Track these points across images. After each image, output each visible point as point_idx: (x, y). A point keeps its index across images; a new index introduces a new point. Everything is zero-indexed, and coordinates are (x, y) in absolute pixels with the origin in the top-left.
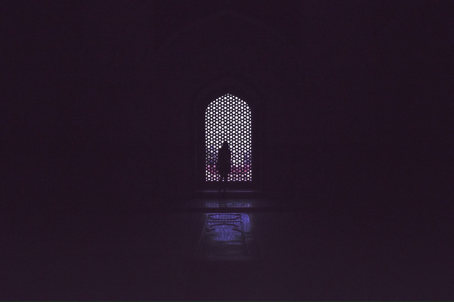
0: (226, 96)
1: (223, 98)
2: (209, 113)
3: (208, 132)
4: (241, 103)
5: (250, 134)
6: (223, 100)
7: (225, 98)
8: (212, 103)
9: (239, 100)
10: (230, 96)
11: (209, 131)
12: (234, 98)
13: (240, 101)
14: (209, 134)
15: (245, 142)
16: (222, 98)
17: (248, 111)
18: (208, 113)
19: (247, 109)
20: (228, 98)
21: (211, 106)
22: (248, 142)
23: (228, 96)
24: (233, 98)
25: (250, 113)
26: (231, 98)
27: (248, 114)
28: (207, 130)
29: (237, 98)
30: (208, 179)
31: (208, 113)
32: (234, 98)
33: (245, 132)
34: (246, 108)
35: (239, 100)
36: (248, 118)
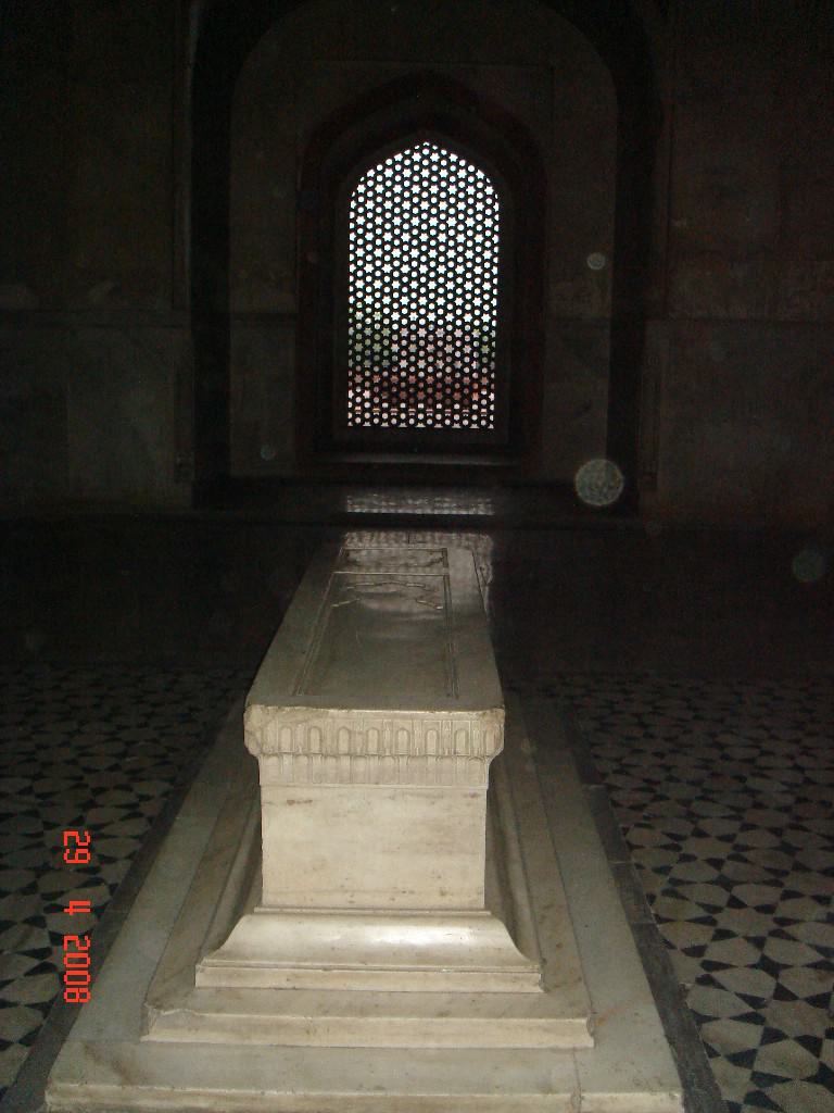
0: (420, 151)
1: (409, 157)
3: (359, 268)
4: (469, 174)
5: (493, 276)
8: (371, 173)
9: (462, 163)
10: (432, 151)
12: (446, 158)
13: (466, 167)
14: (360, 274)
15: (477, 302)
16: (405, 157)
17: (489, 201)
18: (359, 204)
19: (486, 196)
20: (424, 157)
21: (370, 183)
22: (488, 302)
23: (426, 152)
24: (442, 157)
25: (496, 207)
26: (435, 157)
28: (355, 262)
29: (453, 158)
30: (353, 420)
31: (359, 204)
32: (446, 158)
33: (478, 270)
35: (462, 163)
36: (489, 223)
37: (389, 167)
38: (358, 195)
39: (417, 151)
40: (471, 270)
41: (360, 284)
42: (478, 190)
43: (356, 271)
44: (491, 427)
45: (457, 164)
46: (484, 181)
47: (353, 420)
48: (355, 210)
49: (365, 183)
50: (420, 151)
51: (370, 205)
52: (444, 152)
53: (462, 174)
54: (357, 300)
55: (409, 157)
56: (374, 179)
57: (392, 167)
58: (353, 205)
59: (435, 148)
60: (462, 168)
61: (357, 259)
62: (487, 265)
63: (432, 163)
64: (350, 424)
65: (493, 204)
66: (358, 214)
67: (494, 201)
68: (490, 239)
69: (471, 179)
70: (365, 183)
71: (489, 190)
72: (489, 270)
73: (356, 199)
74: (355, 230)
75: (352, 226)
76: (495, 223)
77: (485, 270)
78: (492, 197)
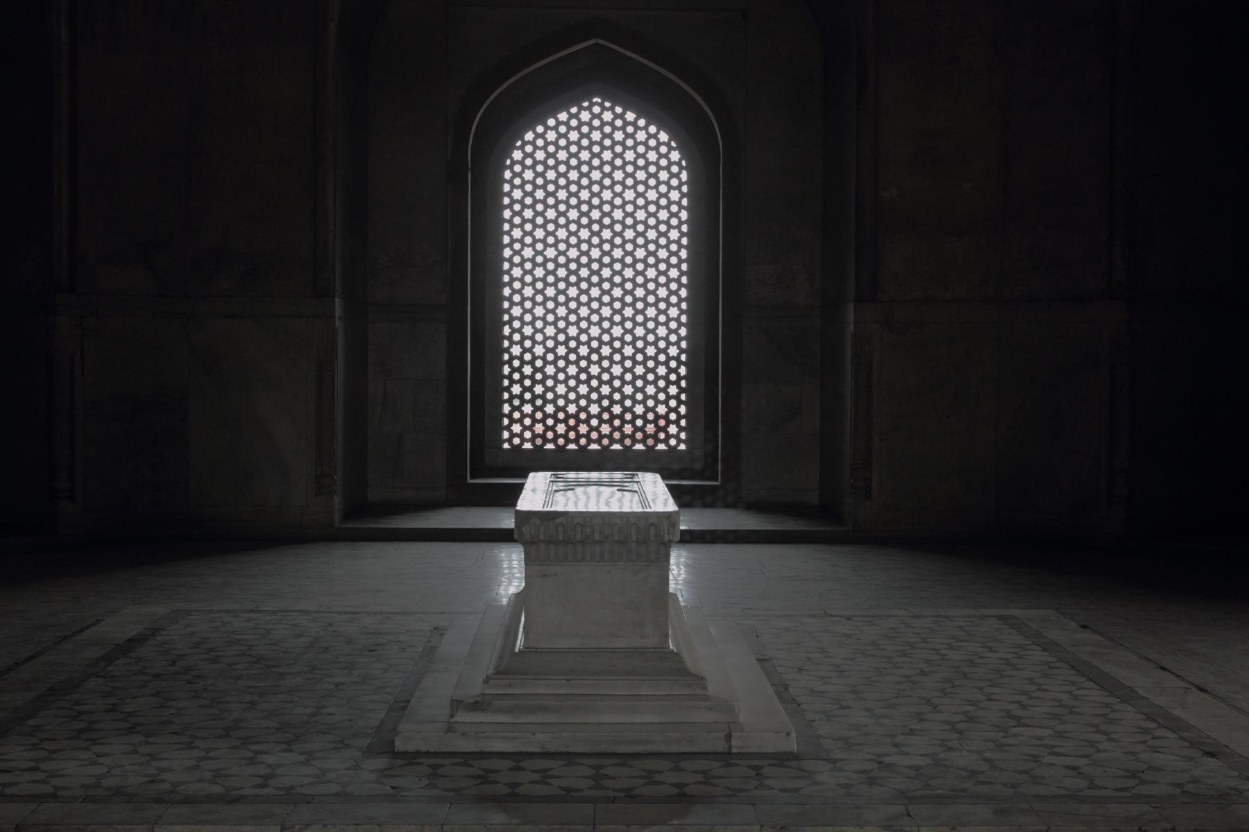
0: (589, 109)
1: (576, 116)
2: (520, 175)
4: (650, 136)
6: (574, 123)
7: (585, 116)
8: (529, 136)
10: (604, 109)
11: (517, 246)
12: (621, 116)
13: (646, 128)
14: (517, 259)
15: (662, 292)
16: (571, 116)
17: (675, 169)
18: (515, 175)
19: (671, 163)
21: (529, 149)
22: (676, 293)
24: (616, 116)
25: (684, 176)
27: (674, 182)
28: (510, 245)
29: (630, 116)
30: (510, 440)
31: (515, 175)
32: (621, 116)
34: (666, 156)
35: (642, 123)
36: (674, 195)
37: (551, 129)
38: (514, 163)
39: (585, 109)
40: (654, 254)
41: (517, 272)
42: (661, 156)
43: (512, 257)
44: (682, 447)
45: (634, 124)
46: (668, 144)
47: (510, 440)
48: (511, 182)
49: (522, 148)
50: (589, 109)
51: (529, 175)
52: (619, 110)
53: (641, 136)
54: (514, 292)
55: (576, 116)
56: (533, 143)
57: (556, 128)
58: (508, 175)
59: (607, 104)
60: (641, 129)
61: (513, 241)
62: (674, 247)
63: (603, 124)
64: (506, 446)
65: (680, 172)
66: (513, 187)
67: (681, 168)
68: (676, 215)
69: (652, 143)
70: (522, 148)
71: (675, 156)
72: (676, 254)
73: (511, 167)
74: (510, 206)
75: (506, 201)
76: (683, 195)
77: (672, 254)
78: (678, 164)
